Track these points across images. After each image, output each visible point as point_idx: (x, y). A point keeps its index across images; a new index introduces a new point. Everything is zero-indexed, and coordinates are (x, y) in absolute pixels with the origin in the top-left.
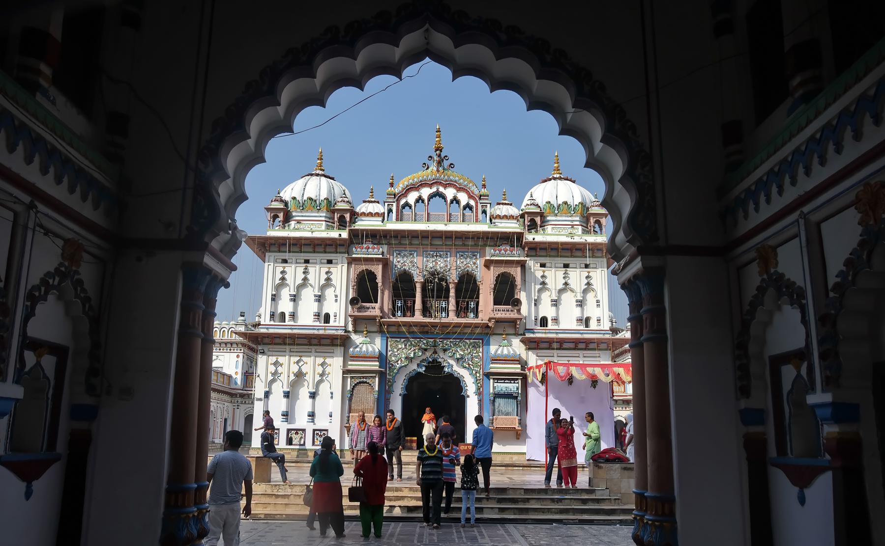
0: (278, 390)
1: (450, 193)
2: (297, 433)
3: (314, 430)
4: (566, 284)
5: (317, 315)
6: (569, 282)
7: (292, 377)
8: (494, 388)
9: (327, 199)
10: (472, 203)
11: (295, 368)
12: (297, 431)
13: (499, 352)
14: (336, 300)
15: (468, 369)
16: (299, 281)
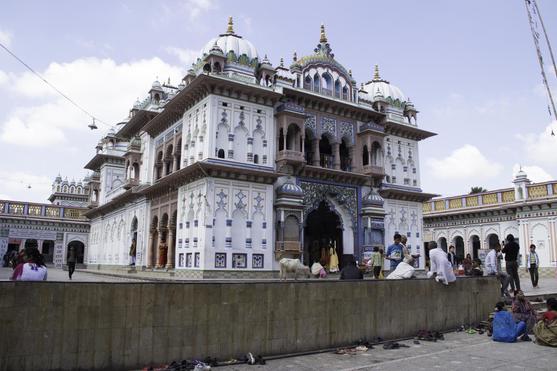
0: (222, 219)
1: (335, 76)
2: (239, 257)
3: (253, 255)
4: (399, 155)
5: (250, 155)
6: (401, 153)
7: (235, 208)
8: (372, 224)
9: (257, 59)
10: (348, 86)
11: (237, 200)
12: (239, 255)
13: (373, 199)
14: (265, 145)
15: (349, 209)
16: (237, 124)
